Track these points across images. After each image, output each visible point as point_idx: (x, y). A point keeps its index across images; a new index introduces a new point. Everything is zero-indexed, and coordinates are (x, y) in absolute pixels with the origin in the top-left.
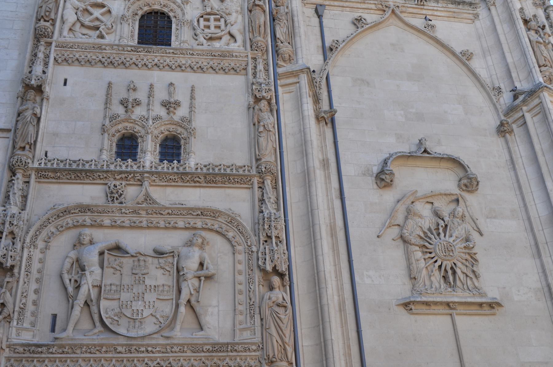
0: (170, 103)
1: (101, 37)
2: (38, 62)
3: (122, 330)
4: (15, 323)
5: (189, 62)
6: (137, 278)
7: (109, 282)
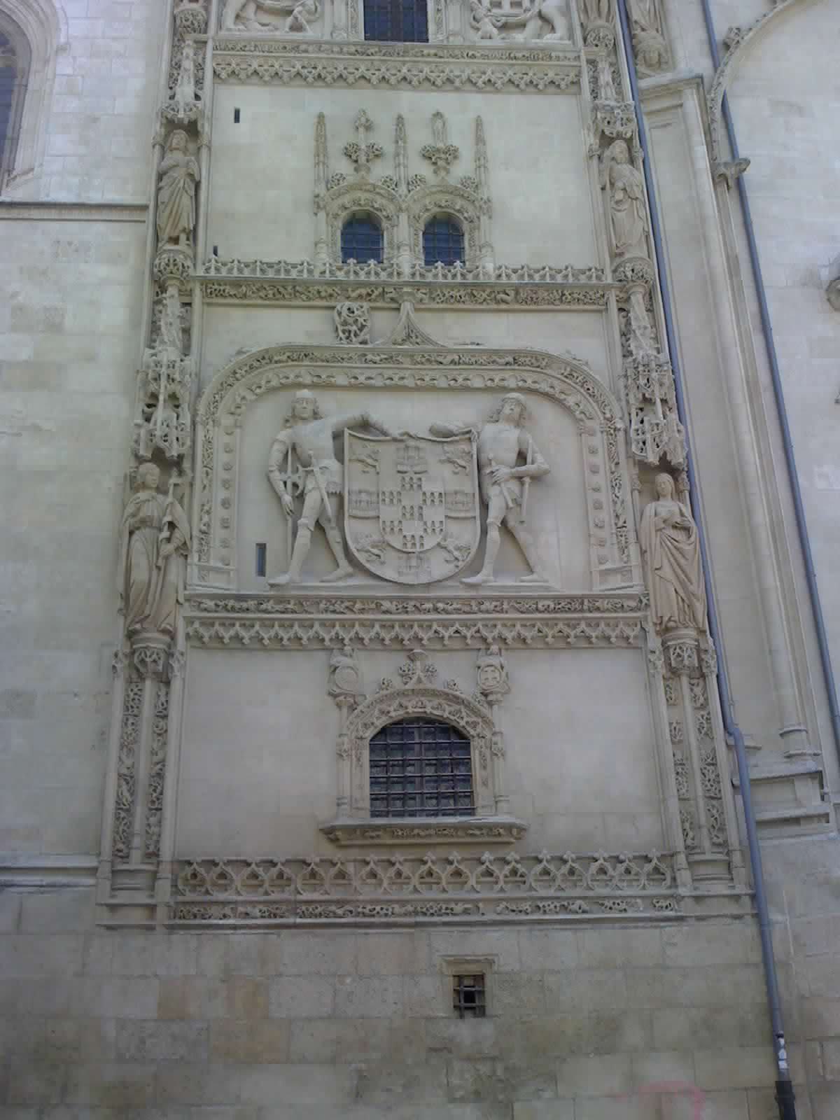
0: (438, 150)
1: (297, 27)
2: (186, 78)
3: (389, 573)
4: (194, 558)
5: (468, 72)
6: (407, 479)
7: (356, 487)
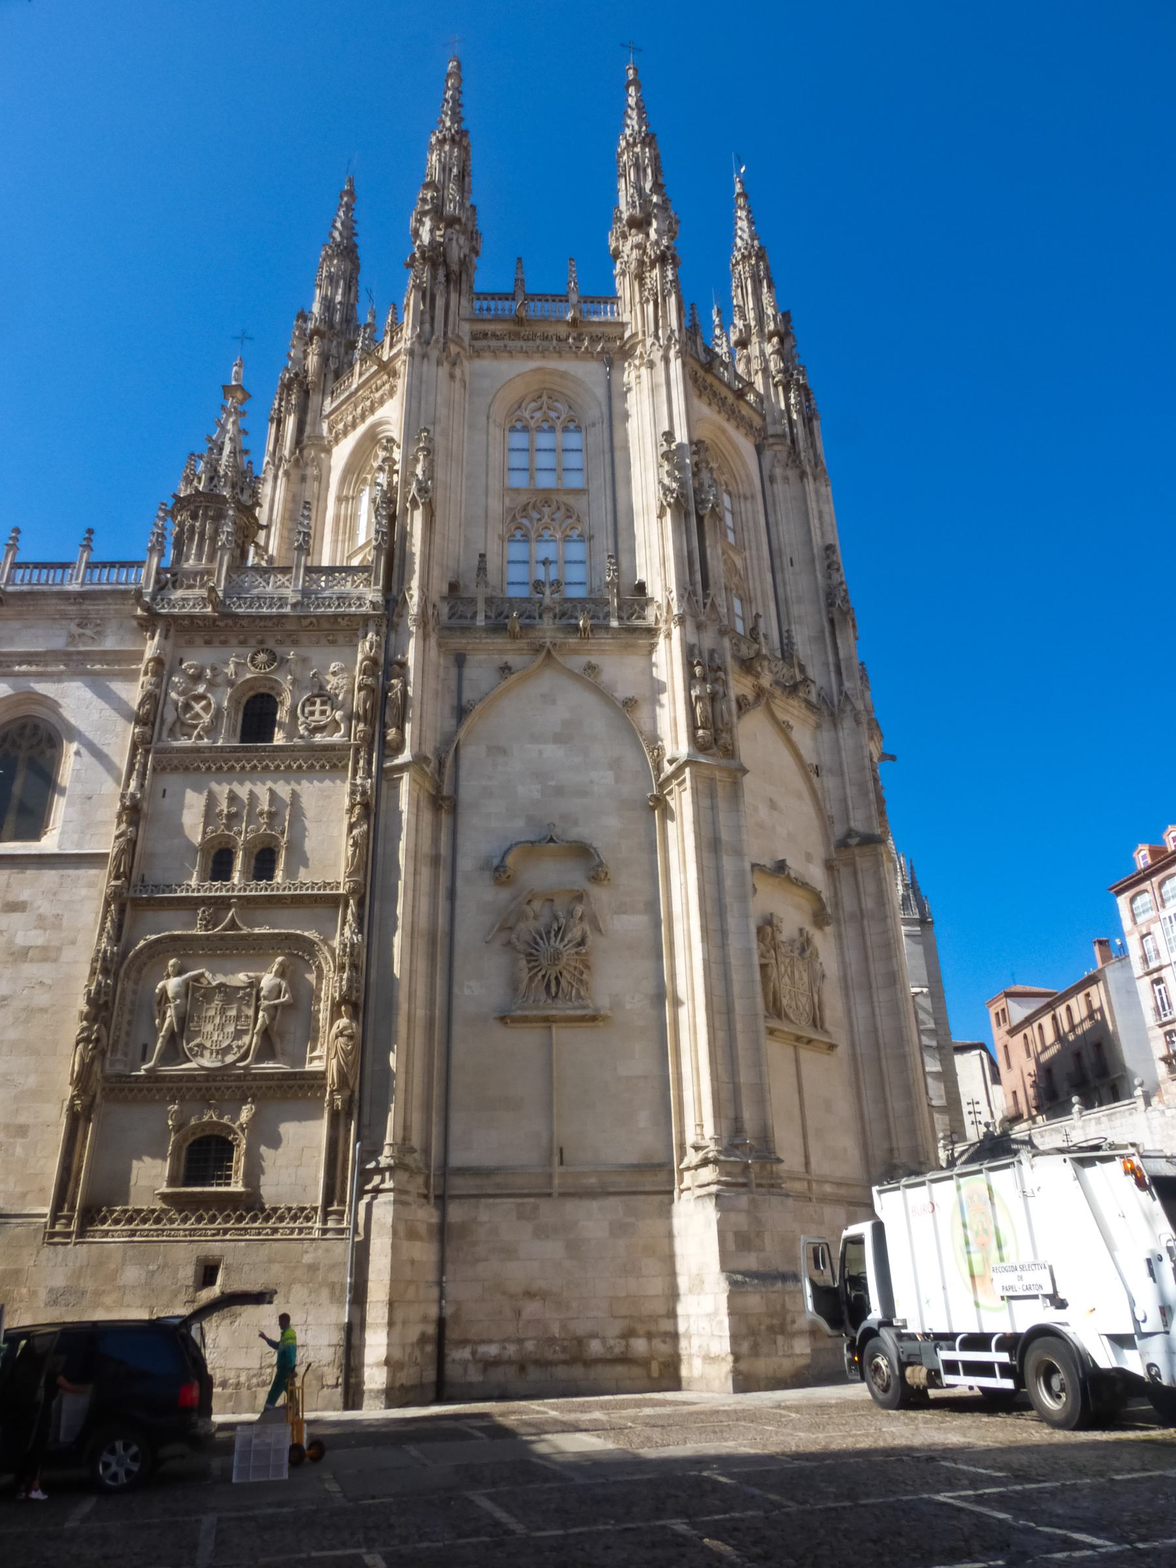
4: (109, 1055)
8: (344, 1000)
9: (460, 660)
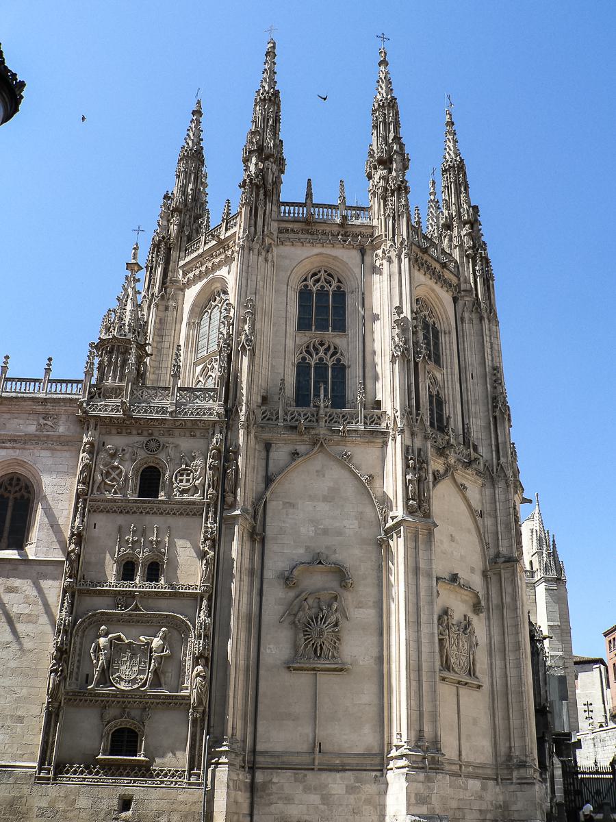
8: (201, 656)
9: (268, 447)
